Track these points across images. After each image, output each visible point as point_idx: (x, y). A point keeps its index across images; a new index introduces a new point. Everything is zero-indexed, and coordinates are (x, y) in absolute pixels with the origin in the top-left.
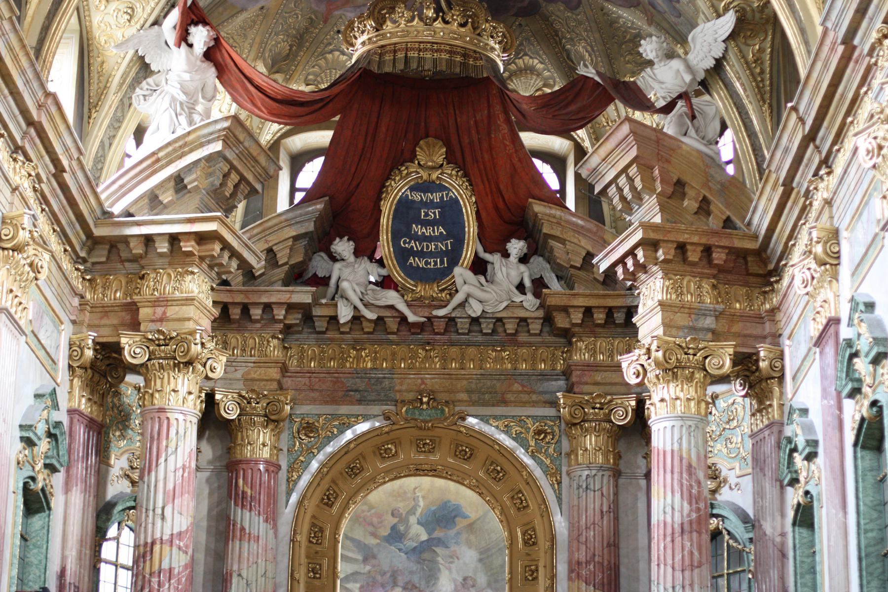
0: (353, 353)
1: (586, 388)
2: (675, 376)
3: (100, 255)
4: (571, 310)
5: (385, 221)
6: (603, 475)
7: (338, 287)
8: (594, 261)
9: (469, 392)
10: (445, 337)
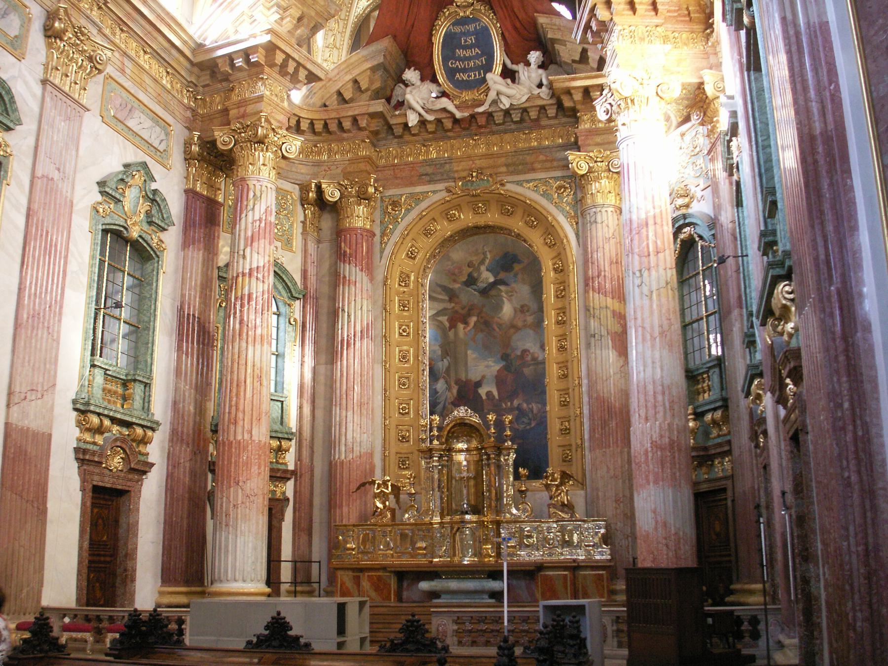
0: (423, 149)
1: (589, 148)
9: (507, 165)
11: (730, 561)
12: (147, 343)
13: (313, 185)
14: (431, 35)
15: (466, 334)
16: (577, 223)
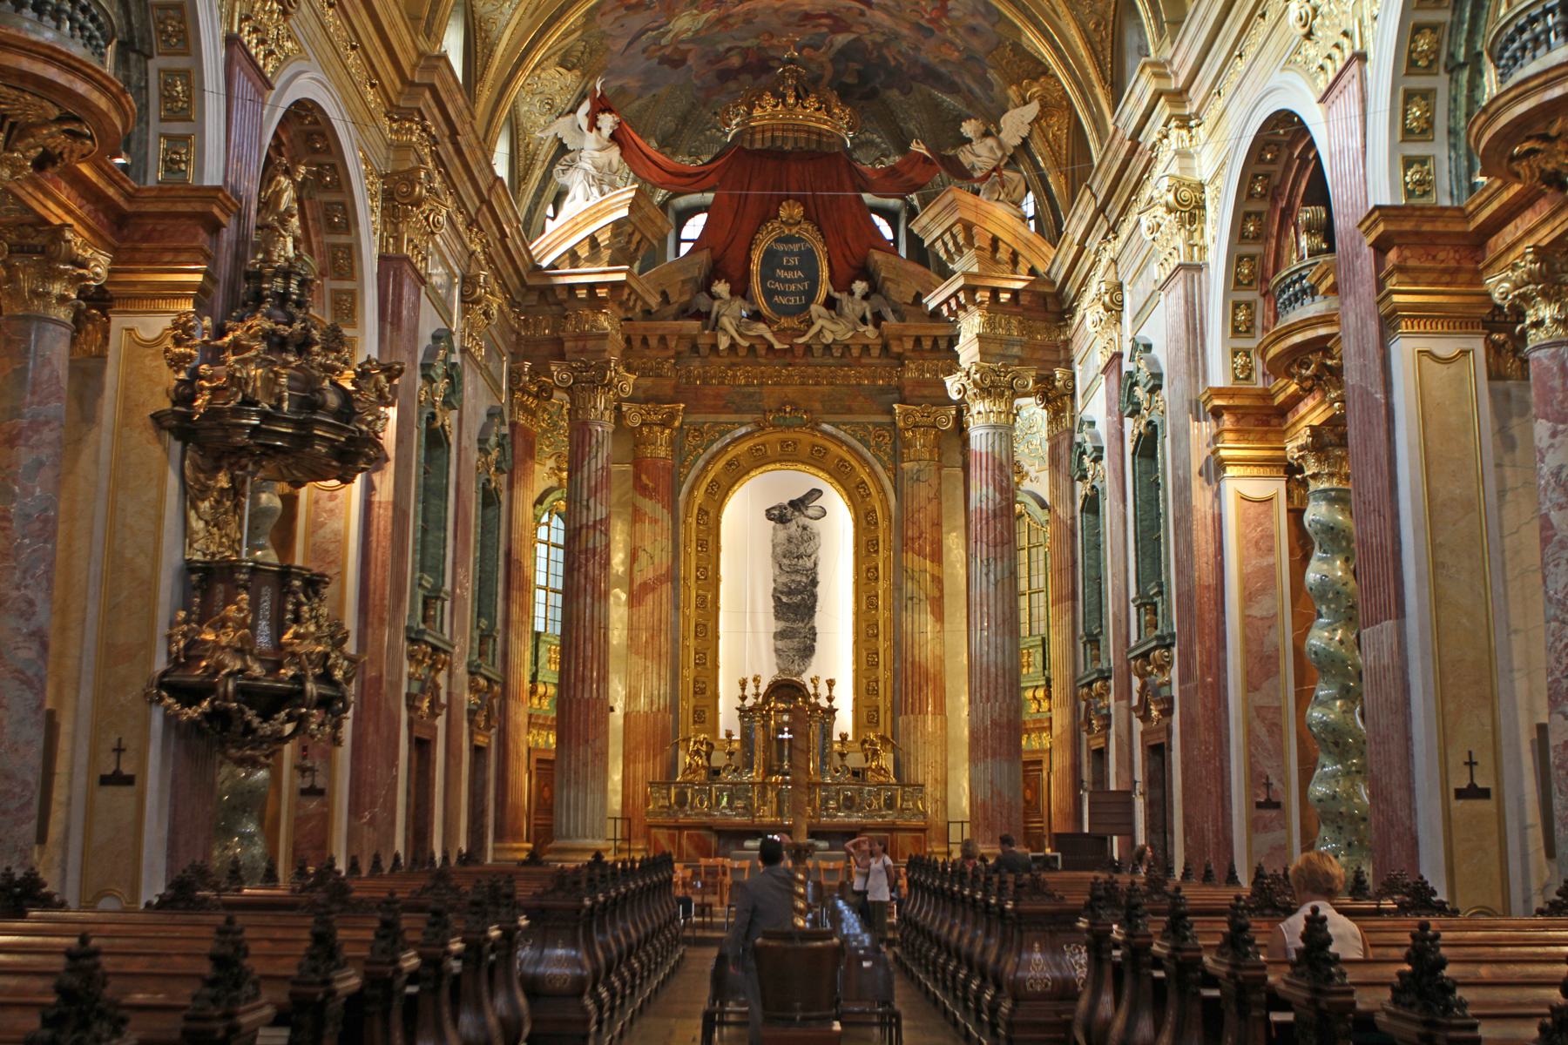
0: (730, 373)
2: (989, 394)
5: (755, 267)
7: (717, 320)
8: (924, 301)
10: (803, 361)
11: (1041, 828)
12: (491, 595)
14: (750, 250)
16: (895, 475)
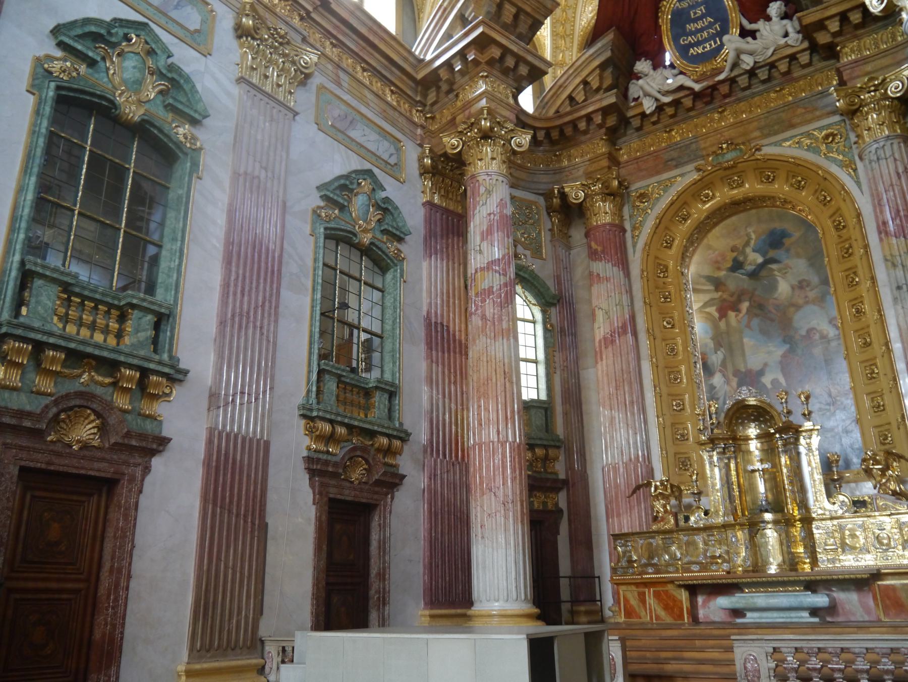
3: (432, 96)
4: (827, 23)
6: (892, 144)
9: (759, 129)
13: (556, 191)
14: (657, 18)
15: (739, 322)
